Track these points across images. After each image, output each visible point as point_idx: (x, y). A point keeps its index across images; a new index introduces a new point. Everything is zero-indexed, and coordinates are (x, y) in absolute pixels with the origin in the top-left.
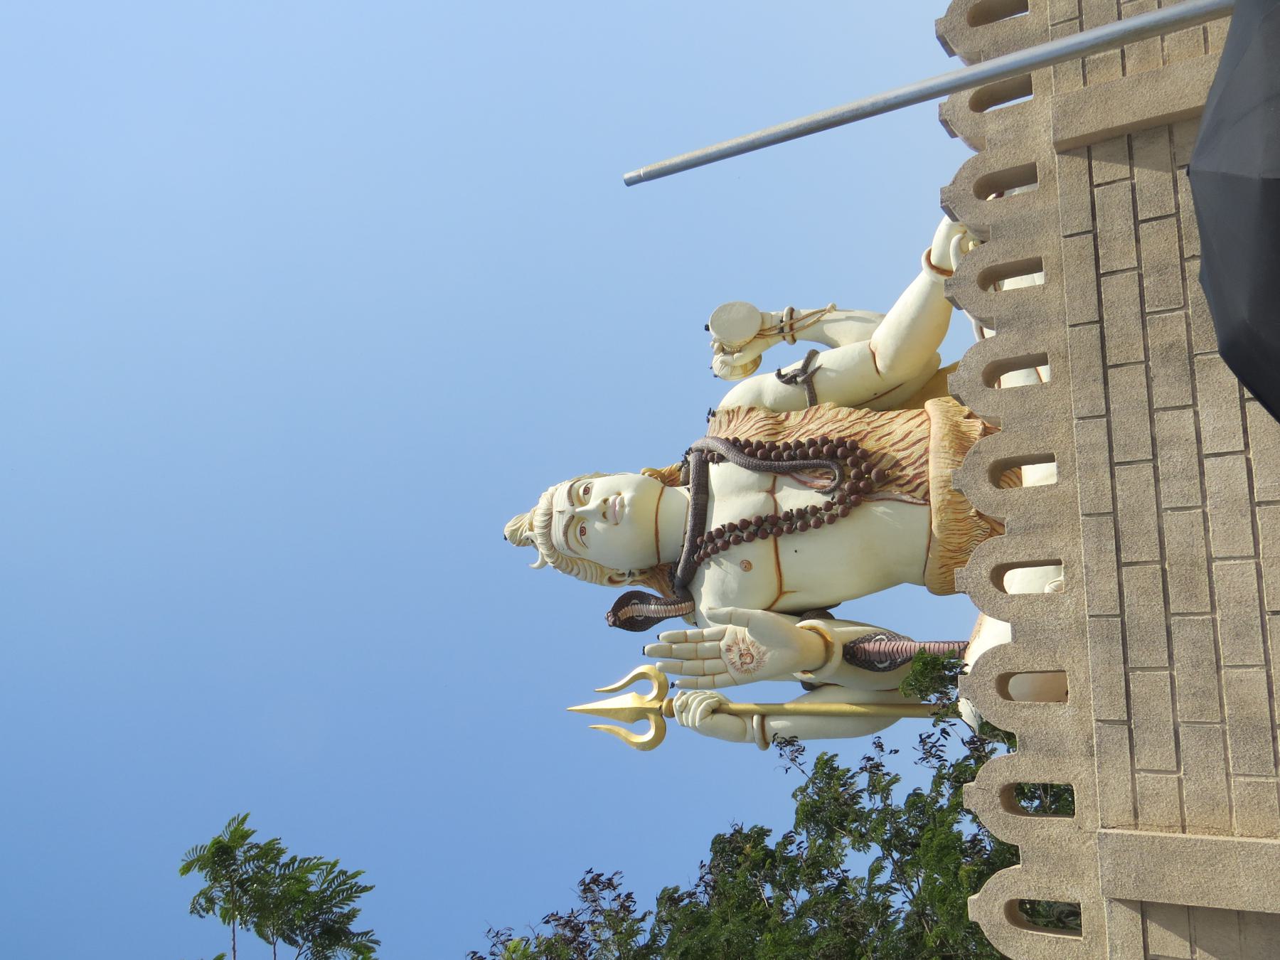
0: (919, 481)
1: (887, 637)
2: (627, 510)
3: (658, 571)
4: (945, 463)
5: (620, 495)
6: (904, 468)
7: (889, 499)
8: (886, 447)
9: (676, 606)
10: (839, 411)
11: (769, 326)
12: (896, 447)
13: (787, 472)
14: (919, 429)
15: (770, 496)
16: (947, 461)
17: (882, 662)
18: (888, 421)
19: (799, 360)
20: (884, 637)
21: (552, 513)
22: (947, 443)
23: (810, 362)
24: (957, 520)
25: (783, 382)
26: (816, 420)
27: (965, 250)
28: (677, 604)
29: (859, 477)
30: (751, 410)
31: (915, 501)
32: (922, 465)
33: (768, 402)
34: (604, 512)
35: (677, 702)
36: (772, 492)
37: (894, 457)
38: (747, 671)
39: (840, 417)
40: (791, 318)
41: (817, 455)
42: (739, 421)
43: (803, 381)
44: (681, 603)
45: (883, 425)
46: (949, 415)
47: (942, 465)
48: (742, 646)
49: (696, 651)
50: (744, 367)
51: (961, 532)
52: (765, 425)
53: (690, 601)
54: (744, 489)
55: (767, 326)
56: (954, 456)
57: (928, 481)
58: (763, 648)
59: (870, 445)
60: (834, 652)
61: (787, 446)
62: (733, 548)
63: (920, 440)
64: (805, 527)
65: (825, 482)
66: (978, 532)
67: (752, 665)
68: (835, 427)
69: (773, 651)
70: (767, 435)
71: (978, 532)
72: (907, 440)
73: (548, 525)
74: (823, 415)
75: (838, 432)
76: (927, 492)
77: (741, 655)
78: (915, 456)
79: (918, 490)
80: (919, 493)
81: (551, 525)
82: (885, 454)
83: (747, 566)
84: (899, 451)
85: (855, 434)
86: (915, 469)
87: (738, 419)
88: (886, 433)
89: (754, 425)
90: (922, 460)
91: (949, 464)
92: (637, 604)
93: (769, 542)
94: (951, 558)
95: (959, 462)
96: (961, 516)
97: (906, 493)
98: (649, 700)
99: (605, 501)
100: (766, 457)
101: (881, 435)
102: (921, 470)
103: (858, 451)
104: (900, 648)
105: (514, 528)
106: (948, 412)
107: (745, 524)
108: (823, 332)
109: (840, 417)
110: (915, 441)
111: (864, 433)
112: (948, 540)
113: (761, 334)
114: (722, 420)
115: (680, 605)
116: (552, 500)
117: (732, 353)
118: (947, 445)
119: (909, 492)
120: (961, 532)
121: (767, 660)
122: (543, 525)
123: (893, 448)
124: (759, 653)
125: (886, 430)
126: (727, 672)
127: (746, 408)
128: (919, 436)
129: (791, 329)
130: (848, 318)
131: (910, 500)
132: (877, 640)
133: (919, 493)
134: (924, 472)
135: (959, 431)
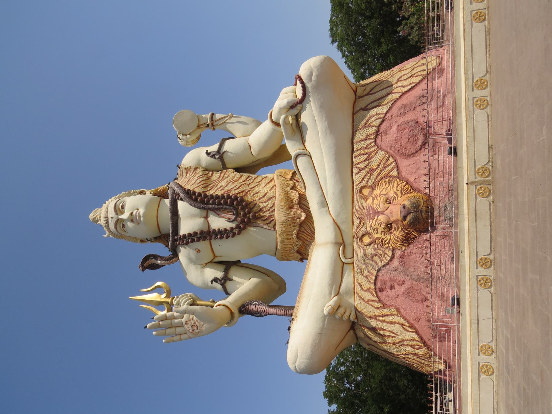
0: (271, 219)
1: (258, 303)
2: (142, 219)
3: (162, 237)
4: (282, 214)
5: (138, 210)
6: (264, 213)
7: (258, 227)
8: (255, 200)
9: (170, 261)
10: (236, 175)
11: (202, 123)
12: (261, 200)
13: (213, 210)
14: (271, 192)
15: (205, 219)
16: (283, 213)
17: (257, 314)
18: (257, 184)
19: (217, 143)
20: (257, 303)
21: (108, 217)
22: (282, 204)
23: (221, 147)
24: (288, 239)
25: (210, 157)
26: (225, 179)
27: (287, 123)
28: (170, 260)
29: (245, 215)
30: (196, 169)
31: (270, 228)
32: (272, 211)
33: (203, 165)
34: (132, 218)
36: (206, 217)
38: (195, 333)
39: (236, 178)
40: (212, 120)
41: (226, 203)
42: (190, 175)
43: (218, 158)
44: (172, 259)
45: (255, 187)
46: (284, 186)
47: (281, 215)
48: (193, 322)
49: (172, 324)
50: (193, 142)
51: (290, 244)
53: (176, 257)
54: (193, 216)
55: (201, 123)
56: (286, 210)
57: (275, 219)
58: (202, 323)
59: (249, 198)
60: (235, 317)
61: (212, 195)
62: (191, 244)
63: (271, 198)
64: (221, 238)
65: (229, 216)
66: (297, 244)
67: (197, 331)
68: (233, 186)
69: (206, 324)
70: (203, 188)
71: (297, 244)
73: (107, 222)
74: (228, 176)
75: (235, 190)
76: (275, 225)
77: (192, 326)
78: (269, 207)
79: (270, 222)
81: (108, 223)
82: (256, 204)
83: (199, 251)
84: (262, 203)
85: (243, 192)
86: (269, 213)
87: (190, 172)
88: (256, 192)
89: (196, 181)
90: (272, 209)
91: (284, 214)
92: (153, 259)
93: (207, 242)
94: (286, 253)
95: (288, 213)
96: (290, 237)
97: (266, 224)
98: (162, 297)
99: (132, 214)
100: (202, 202)
101: (254, 193)
102: (272, 214)
103: (244, 203)
104: (265, 311)
105: (93, 217)
106: (283, 184)
107: (195, 233)
108: (226, 126)
109: (236, 178)
110: (269, 198)
111: (246, 191)
112: (284, 247)
113: (199, 126)
114: (183, 172)
115: (171, 260)
116: (107, 210)
117: (186, 135)
118: (283, 205)
119: (267, 224)
120: (290, 244)
121: (204, 328)
122: (105, 222)
123: (259, 201)
124: (200, 325)
125: (256, 190)
126: (186, 333)
127: (194, 167)
128: (271, 196)
129: (212, 125)
130: (238, 122)
131: (268, 228)
132: (254, 304)
134: (273, 215)
135: (288, 197)
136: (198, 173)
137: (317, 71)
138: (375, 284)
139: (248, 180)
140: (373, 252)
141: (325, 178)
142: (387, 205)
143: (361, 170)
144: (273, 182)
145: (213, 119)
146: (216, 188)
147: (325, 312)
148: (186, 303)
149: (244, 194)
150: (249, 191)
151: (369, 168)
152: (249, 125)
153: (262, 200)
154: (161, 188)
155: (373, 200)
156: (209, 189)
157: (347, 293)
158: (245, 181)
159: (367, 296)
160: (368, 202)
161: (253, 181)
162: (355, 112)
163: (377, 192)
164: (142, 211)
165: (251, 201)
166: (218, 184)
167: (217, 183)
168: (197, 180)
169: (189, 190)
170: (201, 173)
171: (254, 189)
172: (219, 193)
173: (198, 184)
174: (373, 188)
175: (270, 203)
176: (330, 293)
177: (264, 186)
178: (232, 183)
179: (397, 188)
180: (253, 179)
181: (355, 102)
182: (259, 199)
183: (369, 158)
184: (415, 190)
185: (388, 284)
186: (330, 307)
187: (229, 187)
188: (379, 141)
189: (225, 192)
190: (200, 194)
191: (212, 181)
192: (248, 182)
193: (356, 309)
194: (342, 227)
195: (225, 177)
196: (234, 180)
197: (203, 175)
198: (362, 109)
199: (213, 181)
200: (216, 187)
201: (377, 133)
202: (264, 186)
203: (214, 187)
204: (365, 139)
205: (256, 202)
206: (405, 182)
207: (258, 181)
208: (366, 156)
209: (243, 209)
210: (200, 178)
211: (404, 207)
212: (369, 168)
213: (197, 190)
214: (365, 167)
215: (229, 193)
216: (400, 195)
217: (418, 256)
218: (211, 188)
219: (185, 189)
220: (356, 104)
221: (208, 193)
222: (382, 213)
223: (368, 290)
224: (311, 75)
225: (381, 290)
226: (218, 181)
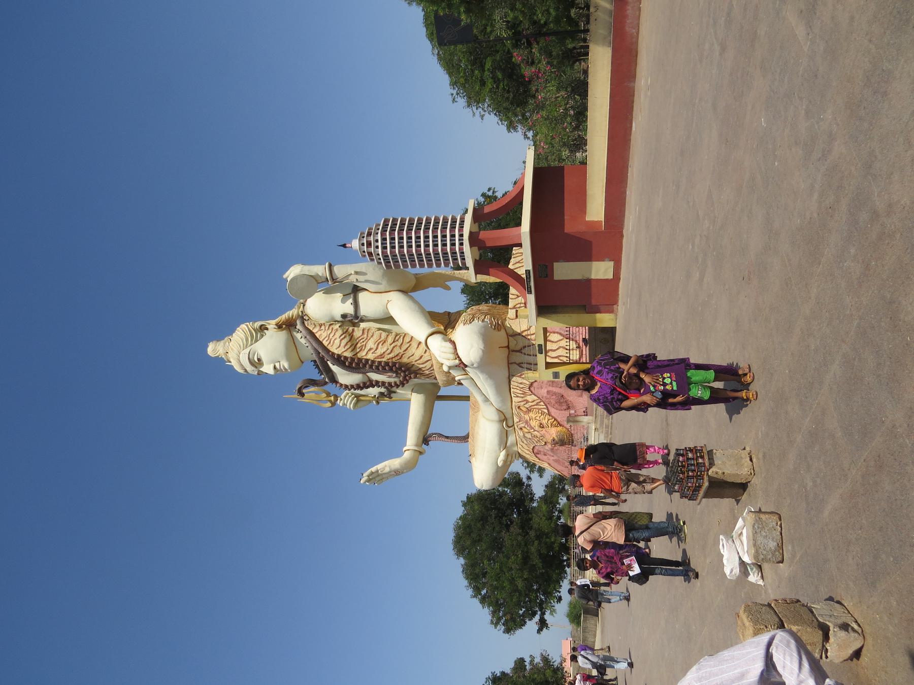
2: (289, 370)
5: (279, 362)
6: (424, 371)
10: (381, 334)
15: (364, 375)
18: (408, 345)
30: (330, 325)
35: (340, 403)
37: (418, 367)
42: (327, 329)
45: (407, 348)
52: (347, 343)
59: (405, 360)
63: (428, 361)
68: (385, 349)
70: (352, 351)
74: (373, 334)
75: (388, 354)
84: (419, 364)
85: (397, 355)
90: (432, 369)
109: (383, 337)
111: (400, 355)
116: (240, 361)
123: (416, 363)
136: (337, 330)
137: (478, 364)
138: (533, 449)
139: (398, 341)
140: (530, 437)
141: (487, 393)
142: (541, 429)
143: (518, 397)
146: (366, 350)
147: (500, 464)
148: (352, 403)
149: (399, 358)
150: (403, 354)
151: (525, 398)
152: (381, 286)
154: (284, 317)
155: (530, 420)
156: (358, 350)
157: (512, 445)
158: (394, 342)
159: (527, 452)
160: (525, 416)
161: (403, 341)
162: (510, 362)
163: (531, 414)
164: (285, 364)
165: (408, 362)
169: (339, 356)
170: (340, 332)
172: (370, 356)
173: (344, 347)
174: (529, 410)
176: (500, 449)
177: (417, 348)
178: (382, 345)
179: (548, 422)
180: (402, 337)
181: (509, 353)
183: (524, 393)
184: (561, 425)
185: (542, 453)
186: (502, 462)
187: (380, 351)
188: (532, 389)
189: (379, 356)
190: (352, 359)
191: (358, 338)
192: (399, 343)
193: (519, 453)
194: (504, 411)
195: (370, 336)
196: (381, 339)
197: (344, 333)
198: (515, 363)
199: (358, 338)
200: (365, 348)
201: (532, 384)
202: (417, 348)
203: (363, 348)
204: (521, 383)
205: (413, 363)
206: (553, 420)
207: (407, 341)
208: (521, 392)
209: (404, 372)
210: (343, 339)
211: (554, 440)
212: (525, 398)
213: (348, 354)
214: (522, 397)
215: (383, 357)
216: (550, 426)
217: (563, 452)
219: (333, 353)
220: (510, 356)
221: (359, 355)
222: (538, 432)
223: (527, 450)
224: (473, 365)
225: (538, 454)
226: (363, 338)
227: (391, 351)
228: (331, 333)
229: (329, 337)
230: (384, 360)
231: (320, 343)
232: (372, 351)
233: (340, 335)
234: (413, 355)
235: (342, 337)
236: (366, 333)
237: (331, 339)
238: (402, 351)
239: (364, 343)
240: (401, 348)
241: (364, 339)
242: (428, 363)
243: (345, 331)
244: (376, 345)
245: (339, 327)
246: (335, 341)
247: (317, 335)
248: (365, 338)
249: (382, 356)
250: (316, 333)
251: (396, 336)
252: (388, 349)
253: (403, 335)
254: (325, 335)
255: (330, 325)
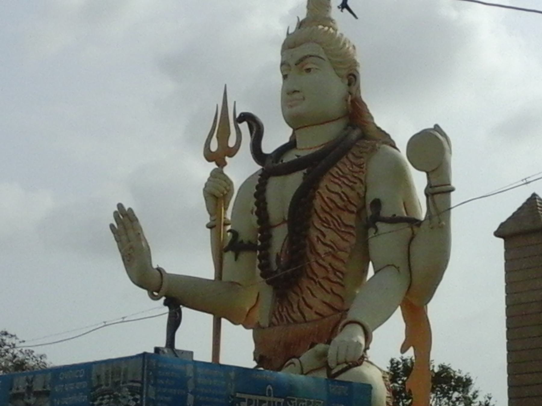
8: (302, 293)
32: (287, 320)
42: (356, 175)
59: (305, 283)
70: (322, 208)
72: (305, 307)
74: (347, 241)
80: (274, 320)
85: (313, 272)
86: (286, 317)
101: (312, 289)
111: (315, 278)
123: (301, 299)
127: (363, 179)
133: (274, 320)
136: (352, 188)
139: (335, 274)
144: (331, 312)
145: (435, 196)
146: (323, 229)
149: (311, 275)
153: (302, 304)
166: (331, 228)
167: (334, 225)
168: (337, 193)
171: (318, 285)
172: (314, 234)
175: (297, 316)
180: (339, 280)
182: (303, 298)
187: (321, 249)
192: (332, 276)
203: (325, 225)
207: (334, 289)
213: (317, 203)
215: (311, 252)
218: (324, 219)
226: (339, 224)
227: (320, 265)
228: (351, 181)
229: (342, 177)
230: (308, 253)
231: (333, 164)
232: (320, 236)
233: (346, 193)
234: (312, 294)
235: (343, 195)
236: (346, 230)
237: (340, 180)
238: (320, 280)
239: (332, 226)
240: (323, 278)
241: (336, 224)
242: (299, 314)
243: (351, 200)
244: (329, 243)
245: (358, 194)
246: (337, 186)
247: (344, 159)
248: (339, 228)
249: (314, 250)
250: (347, 158)
251: (342, 273)
252: (324, 260)
253: (343, 283)
254: (346, 171)
255: (361, 180)
